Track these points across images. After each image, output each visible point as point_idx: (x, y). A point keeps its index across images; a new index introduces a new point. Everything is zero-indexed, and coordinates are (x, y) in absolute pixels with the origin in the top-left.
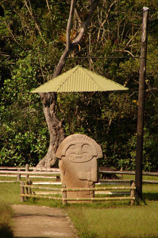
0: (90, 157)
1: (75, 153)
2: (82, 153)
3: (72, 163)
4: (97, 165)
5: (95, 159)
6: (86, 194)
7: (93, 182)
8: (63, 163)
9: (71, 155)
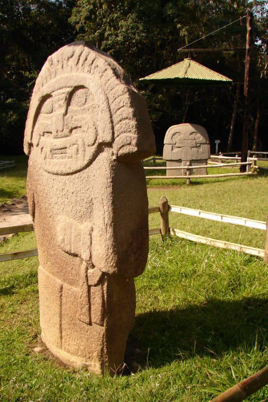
0: (87, 148)
1: (51, 133)
2: (66, 131)
4: (110, 190)
5: (106, 157)
7: (100, 273)
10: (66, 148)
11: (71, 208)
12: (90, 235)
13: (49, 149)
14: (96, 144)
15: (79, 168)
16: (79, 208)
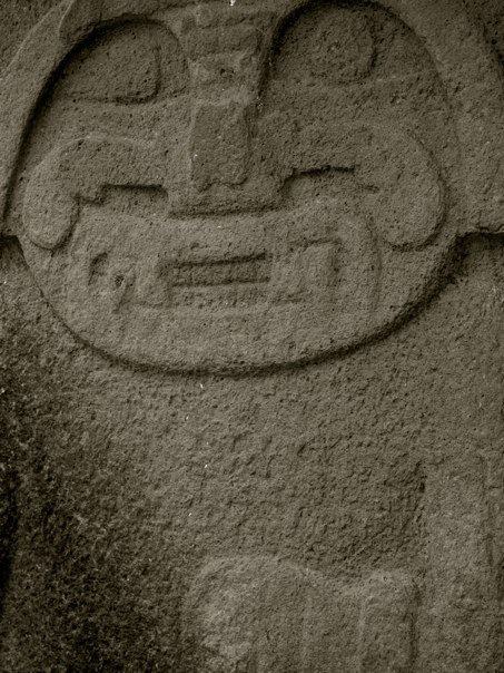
1: (156, 190)
9: (92, 216)
10: (262, 257)
11: (289, 517)
13: (154, 261)
14: (444, 244)
15: (346, 343)
16: (342, 511)
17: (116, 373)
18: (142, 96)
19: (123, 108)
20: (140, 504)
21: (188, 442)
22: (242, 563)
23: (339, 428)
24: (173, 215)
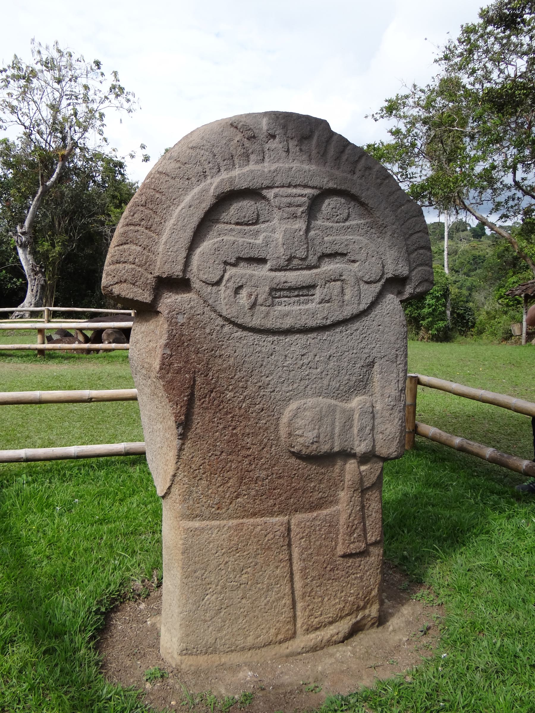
1: (263, 261)
2: (312, 259)
3: (240, 333)
6: (344, 556)
8: (171, 336)
9: (231, 271)
11: (326, 382)
12: (372, 412)
13: (267, 289)
14: (383, 281)
16: (346, 378)
17: (245, 333)
18: (250, 222)
19: (239, 227)
20: (260, 384)
21: (281, 358)
22: (310, 401)
23: (345, 348)
24: (271, 270)
